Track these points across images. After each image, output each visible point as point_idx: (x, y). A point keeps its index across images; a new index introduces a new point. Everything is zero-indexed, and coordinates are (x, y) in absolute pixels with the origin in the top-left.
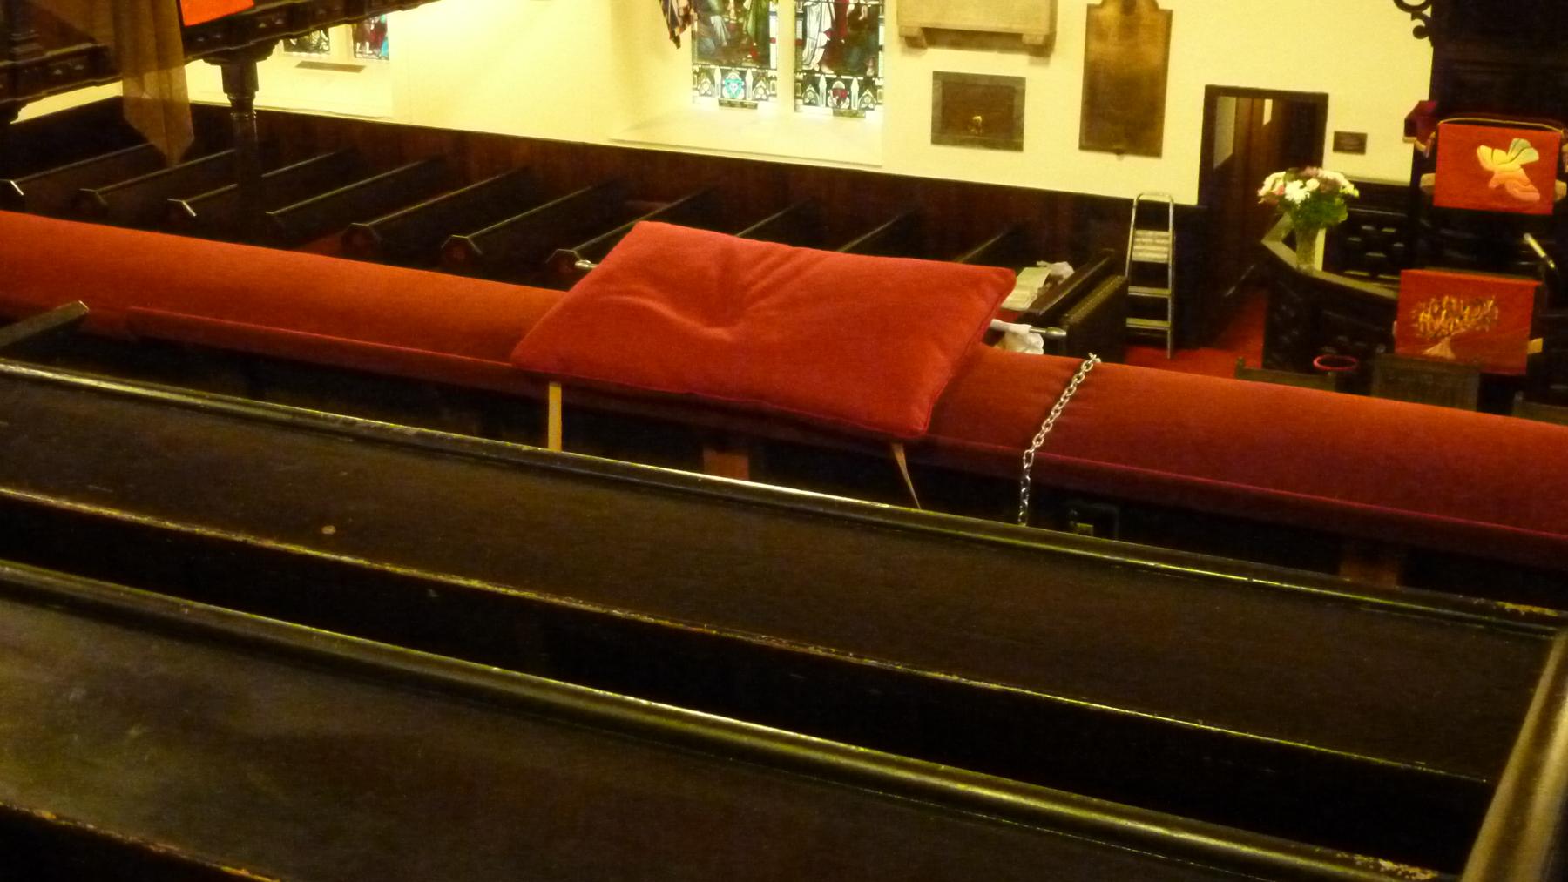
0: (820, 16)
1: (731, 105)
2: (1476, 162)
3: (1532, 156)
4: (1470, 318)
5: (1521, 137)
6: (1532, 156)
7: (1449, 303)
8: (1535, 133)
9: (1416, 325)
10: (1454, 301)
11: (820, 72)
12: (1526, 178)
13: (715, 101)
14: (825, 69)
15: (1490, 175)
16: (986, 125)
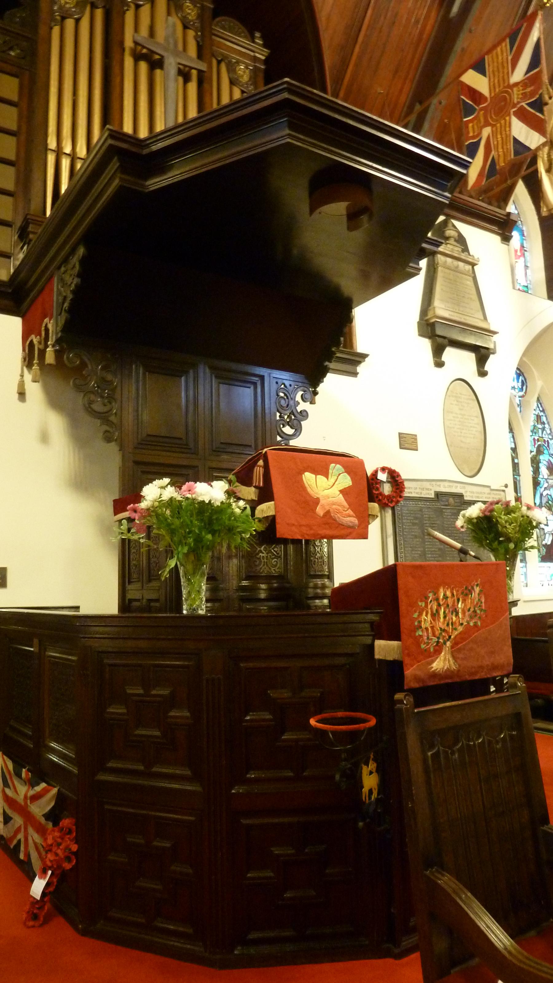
2: (302, 487)
3: (346, 481)
5: (336, 463)
7: (445, 597)
10: (449, 593)
15: (317, 501)
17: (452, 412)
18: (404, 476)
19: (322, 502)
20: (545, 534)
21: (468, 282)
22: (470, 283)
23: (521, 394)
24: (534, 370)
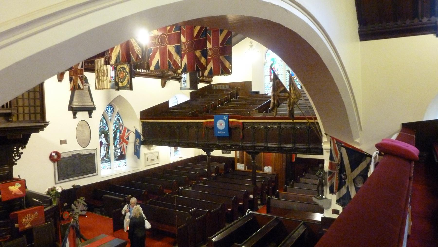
2: (9, 190)
3: (20, 186)
4: (33, 217)
6: (20, 186)
7: (29, 215)
8: (19, 181)
9: (22, 223)
12: (19, 190)
15: (12, 192)
17: (79, 130)
18: (60, 152)
19: (13, 191)
20: (118, 153)
21: (87, 91)
22: (87, 92)
23: (111, 113)
24: (116, 106)
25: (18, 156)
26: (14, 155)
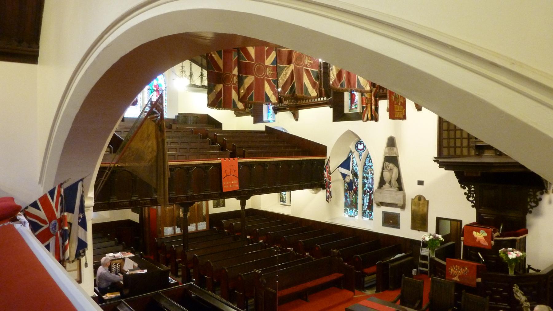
0: (366, 199)
1: (350, 216)
3: (486, 234)
5: (483, 230)
6: (486, 234)
8: (486, 229)
9: (450, 272)
11: (366, 211)
12: (484, 240)
13: (348, 215)
14: (367, 210)
15: (476, 238)
16: (393, 223)
25: (534, 202)
26: (529, 200)
